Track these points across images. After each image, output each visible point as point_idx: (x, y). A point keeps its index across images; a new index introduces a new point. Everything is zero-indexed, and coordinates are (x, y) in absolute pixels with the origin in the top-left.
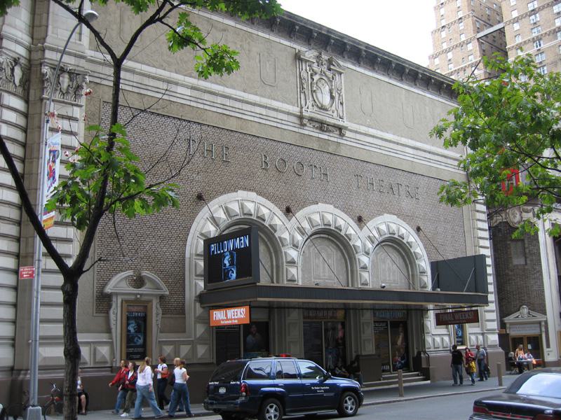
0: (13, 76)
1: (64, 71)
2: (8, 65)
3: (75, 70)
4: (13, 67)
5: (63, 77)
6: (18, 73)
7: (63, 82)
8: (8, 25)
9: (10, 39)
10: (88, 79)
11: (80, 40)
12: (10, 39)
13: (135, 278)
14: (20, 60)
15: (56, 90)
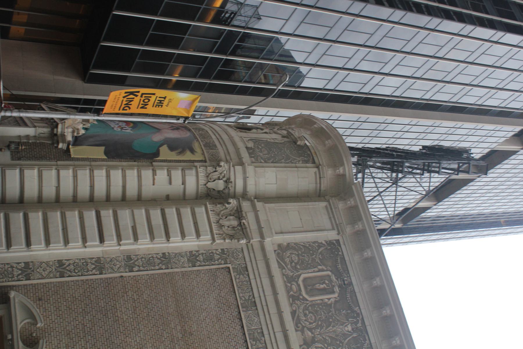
0: (214, 181)
1: (239, 218)
2: (221, 173)
3: (246, 228)
4: (222, 179)
5: (234, 220)
6: (220, 185)
7: (229, 220)
8: (255, 171)
9: (244, 172)
10: (243, 242)
11: (276, 233)
12: (244, 172)
13: (34, 335)
14: (230, 184)
15: (218, 215)
